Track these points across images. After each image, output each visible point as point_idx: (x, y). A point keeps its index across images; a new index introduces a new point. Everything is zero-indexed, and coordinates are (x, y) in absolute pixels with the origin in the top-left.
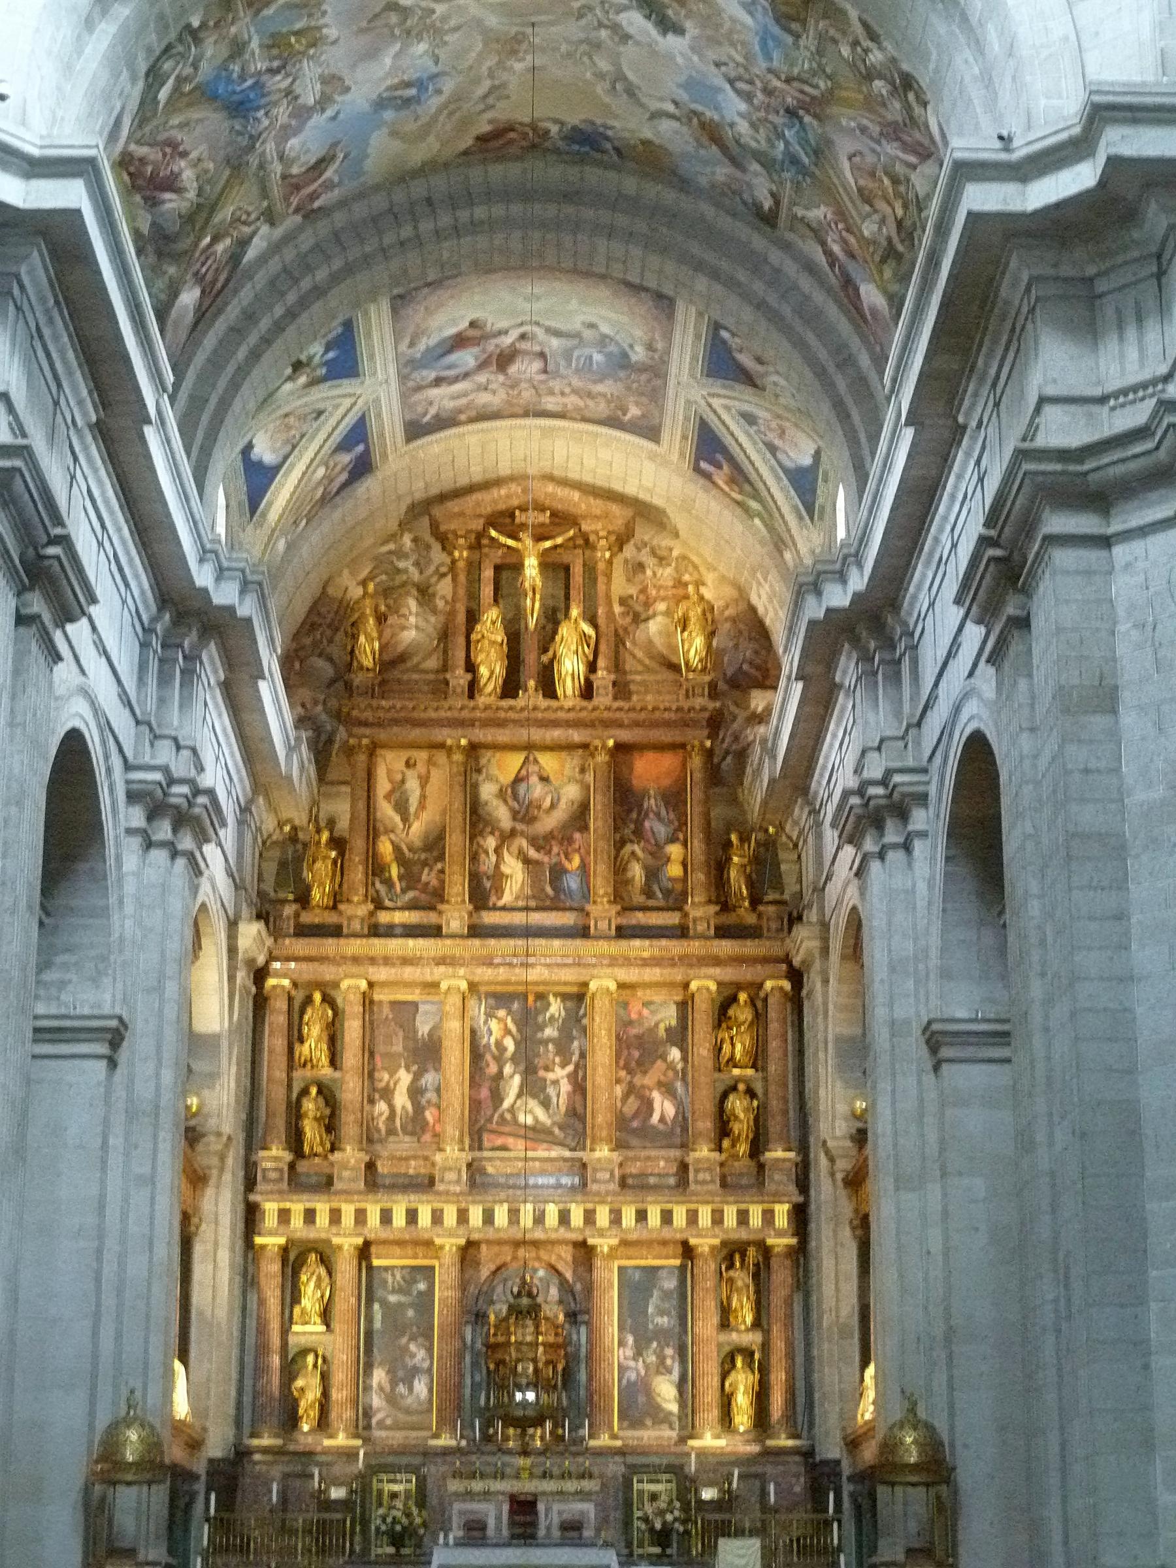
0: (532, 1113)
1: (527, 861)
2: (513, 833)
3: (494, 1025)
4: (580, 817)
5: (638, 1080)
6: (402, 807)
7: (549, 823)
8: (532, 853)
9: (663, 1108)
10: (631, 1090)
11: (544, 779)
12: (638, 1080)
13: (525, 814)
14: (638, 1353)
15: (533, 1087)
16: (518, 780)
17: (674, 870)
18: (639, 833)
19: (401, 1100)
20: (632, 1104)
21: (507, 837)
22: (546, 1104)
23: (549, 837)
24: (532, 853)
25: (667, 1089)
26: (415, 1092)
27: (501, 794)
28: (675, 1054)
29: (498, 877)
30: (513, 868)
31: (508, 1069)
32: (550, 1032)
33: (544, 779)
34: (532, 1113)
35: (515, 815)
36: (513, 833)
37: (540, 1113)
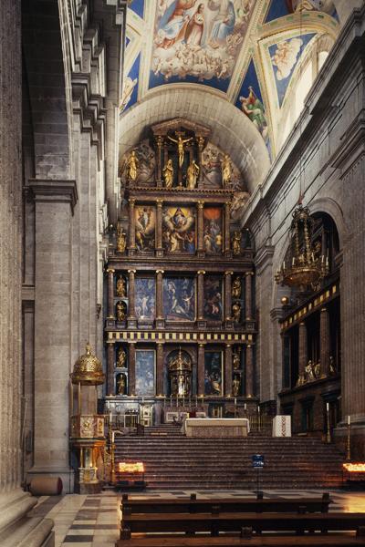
0: (180, 310)
1: (178, 239)
2: (174, 231)
3: (170, 286)
4: (193, 226)
5: (209, 301)
6: (143, 223)
7: (184, 228)
8: (179, 237)
9: (215, 309)
10: (207, 304)
11: (183, 216)
12: (209, 301)
13: (177, 225)
14: (209, 375)
15: (181, 303)
16: (175, 216)
17: (219, 243)
18: (209, 232)
19: (144, 306)
20: (207, 308)
21: (172, 232)
22: (184, 308)
23: (184, 232)
24: (179, 237)
25: (217, 305)
26: (148, 303)
27: (171, 220)
28: (219, 294)
29: (170, 244)
30: (174, 241)
31: (173, 298)
32: (184, 288)
33: (183, 216)
34: (180, 310)
35: (175, 226)
36: (174, 231)
37: (182, 310)
